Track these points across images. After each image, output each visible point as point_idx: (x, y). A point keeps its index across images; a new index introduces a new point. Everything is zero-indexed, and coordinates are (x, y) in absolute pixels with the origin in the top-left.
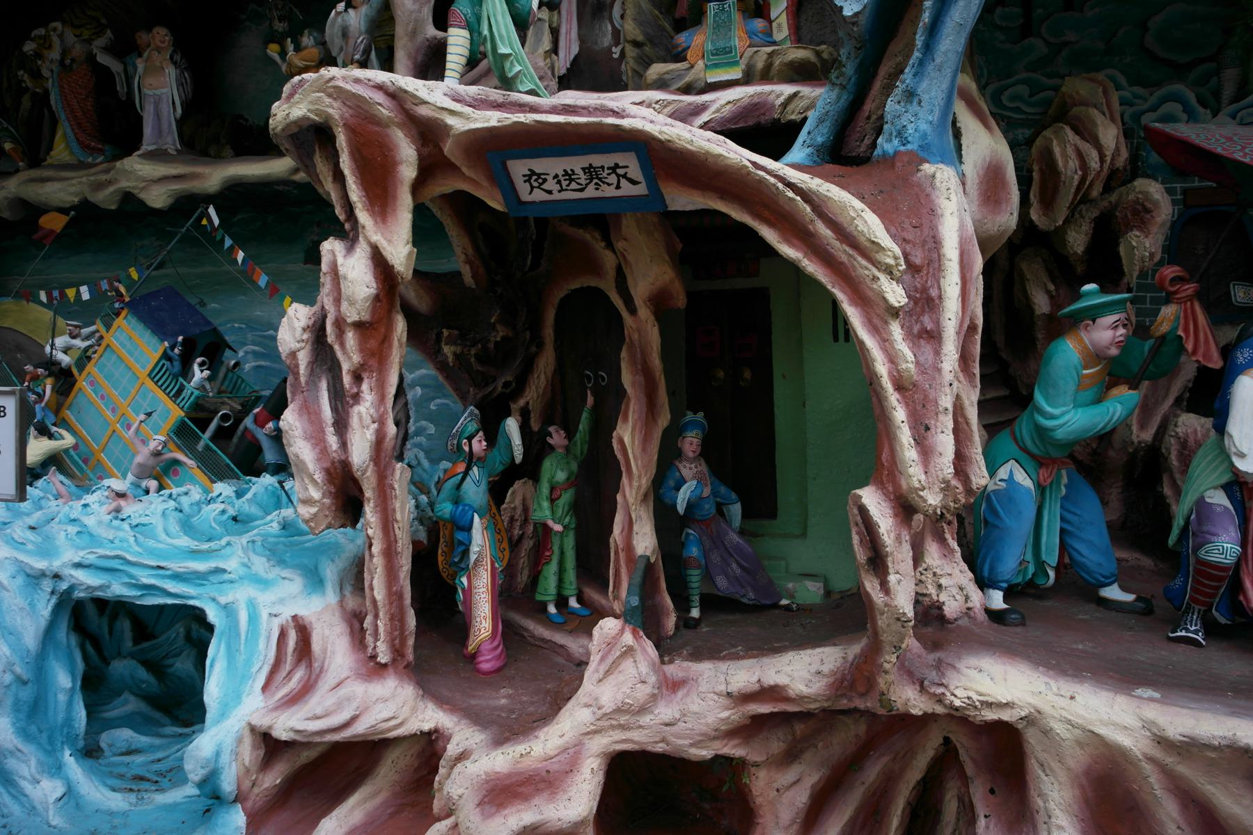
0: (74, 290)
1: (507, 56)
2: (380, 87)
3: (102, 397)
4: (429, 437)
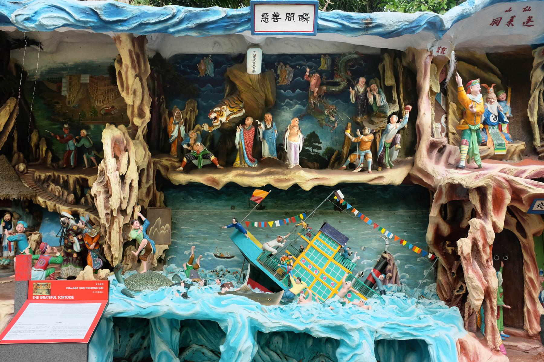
0: (272, 222)
1: (476, 154)
2: (504, 178)
3: (310, 267)
4: (408, 279)
